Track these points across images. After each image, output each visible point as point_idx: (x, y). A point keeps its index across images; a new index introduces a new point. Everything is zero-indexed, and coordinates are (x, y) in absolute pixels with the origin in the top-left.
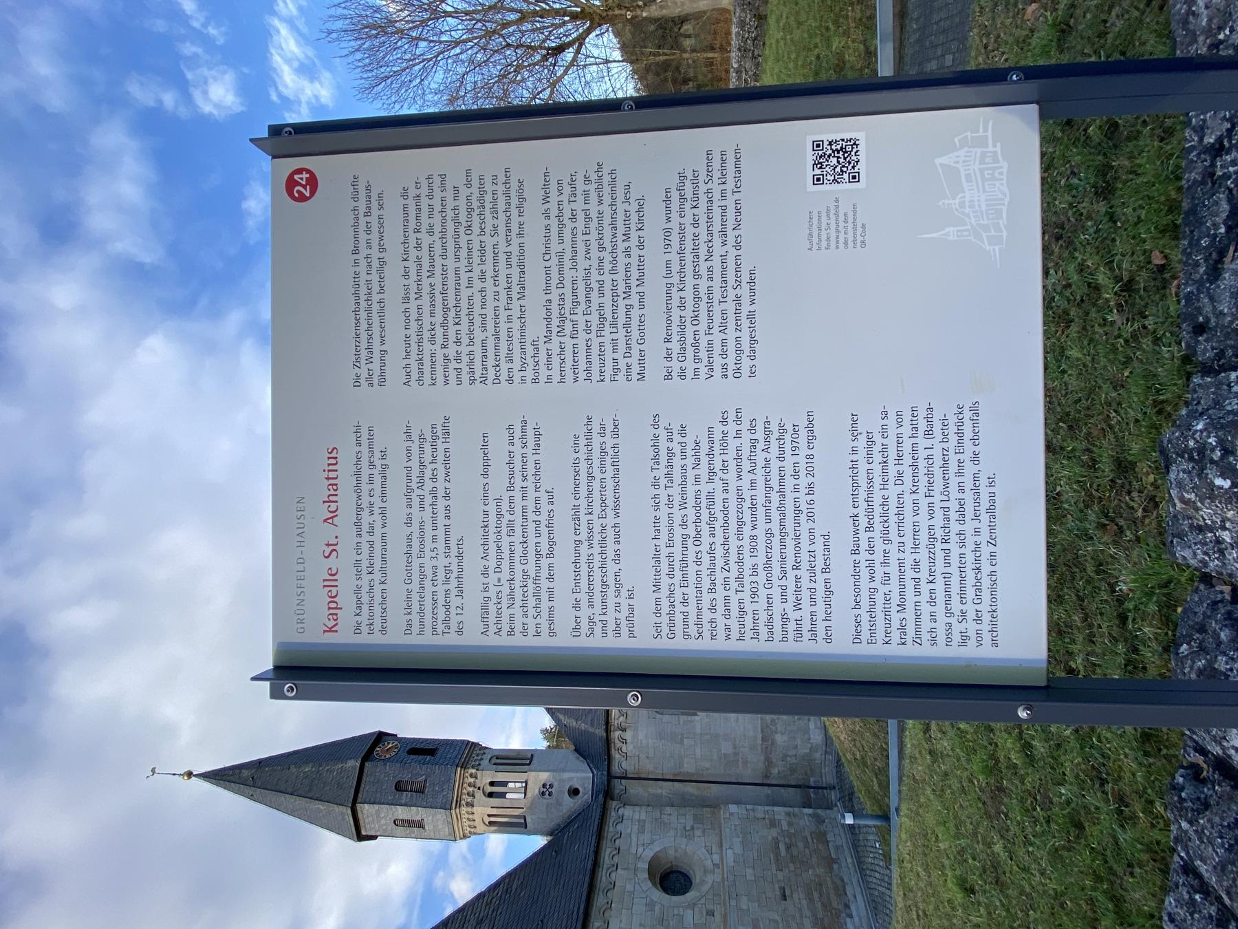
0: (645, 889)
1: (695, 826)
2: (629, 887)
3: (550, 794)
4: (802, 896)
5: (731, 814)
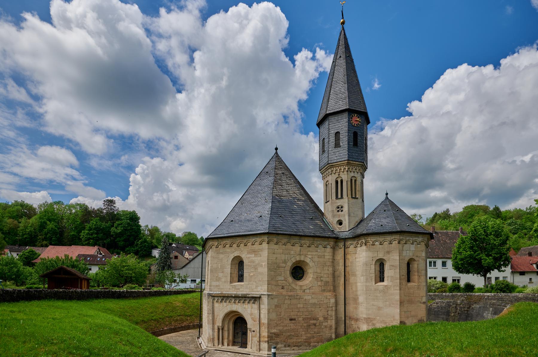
0: (292, 259)
1: (323, 282)
2: (292, 252)
3: (338, 211)
4: (292, 327)
5: (329, 299)
